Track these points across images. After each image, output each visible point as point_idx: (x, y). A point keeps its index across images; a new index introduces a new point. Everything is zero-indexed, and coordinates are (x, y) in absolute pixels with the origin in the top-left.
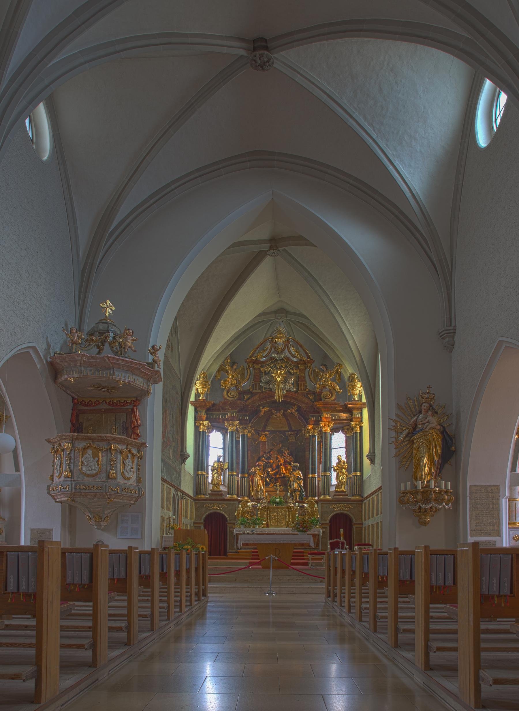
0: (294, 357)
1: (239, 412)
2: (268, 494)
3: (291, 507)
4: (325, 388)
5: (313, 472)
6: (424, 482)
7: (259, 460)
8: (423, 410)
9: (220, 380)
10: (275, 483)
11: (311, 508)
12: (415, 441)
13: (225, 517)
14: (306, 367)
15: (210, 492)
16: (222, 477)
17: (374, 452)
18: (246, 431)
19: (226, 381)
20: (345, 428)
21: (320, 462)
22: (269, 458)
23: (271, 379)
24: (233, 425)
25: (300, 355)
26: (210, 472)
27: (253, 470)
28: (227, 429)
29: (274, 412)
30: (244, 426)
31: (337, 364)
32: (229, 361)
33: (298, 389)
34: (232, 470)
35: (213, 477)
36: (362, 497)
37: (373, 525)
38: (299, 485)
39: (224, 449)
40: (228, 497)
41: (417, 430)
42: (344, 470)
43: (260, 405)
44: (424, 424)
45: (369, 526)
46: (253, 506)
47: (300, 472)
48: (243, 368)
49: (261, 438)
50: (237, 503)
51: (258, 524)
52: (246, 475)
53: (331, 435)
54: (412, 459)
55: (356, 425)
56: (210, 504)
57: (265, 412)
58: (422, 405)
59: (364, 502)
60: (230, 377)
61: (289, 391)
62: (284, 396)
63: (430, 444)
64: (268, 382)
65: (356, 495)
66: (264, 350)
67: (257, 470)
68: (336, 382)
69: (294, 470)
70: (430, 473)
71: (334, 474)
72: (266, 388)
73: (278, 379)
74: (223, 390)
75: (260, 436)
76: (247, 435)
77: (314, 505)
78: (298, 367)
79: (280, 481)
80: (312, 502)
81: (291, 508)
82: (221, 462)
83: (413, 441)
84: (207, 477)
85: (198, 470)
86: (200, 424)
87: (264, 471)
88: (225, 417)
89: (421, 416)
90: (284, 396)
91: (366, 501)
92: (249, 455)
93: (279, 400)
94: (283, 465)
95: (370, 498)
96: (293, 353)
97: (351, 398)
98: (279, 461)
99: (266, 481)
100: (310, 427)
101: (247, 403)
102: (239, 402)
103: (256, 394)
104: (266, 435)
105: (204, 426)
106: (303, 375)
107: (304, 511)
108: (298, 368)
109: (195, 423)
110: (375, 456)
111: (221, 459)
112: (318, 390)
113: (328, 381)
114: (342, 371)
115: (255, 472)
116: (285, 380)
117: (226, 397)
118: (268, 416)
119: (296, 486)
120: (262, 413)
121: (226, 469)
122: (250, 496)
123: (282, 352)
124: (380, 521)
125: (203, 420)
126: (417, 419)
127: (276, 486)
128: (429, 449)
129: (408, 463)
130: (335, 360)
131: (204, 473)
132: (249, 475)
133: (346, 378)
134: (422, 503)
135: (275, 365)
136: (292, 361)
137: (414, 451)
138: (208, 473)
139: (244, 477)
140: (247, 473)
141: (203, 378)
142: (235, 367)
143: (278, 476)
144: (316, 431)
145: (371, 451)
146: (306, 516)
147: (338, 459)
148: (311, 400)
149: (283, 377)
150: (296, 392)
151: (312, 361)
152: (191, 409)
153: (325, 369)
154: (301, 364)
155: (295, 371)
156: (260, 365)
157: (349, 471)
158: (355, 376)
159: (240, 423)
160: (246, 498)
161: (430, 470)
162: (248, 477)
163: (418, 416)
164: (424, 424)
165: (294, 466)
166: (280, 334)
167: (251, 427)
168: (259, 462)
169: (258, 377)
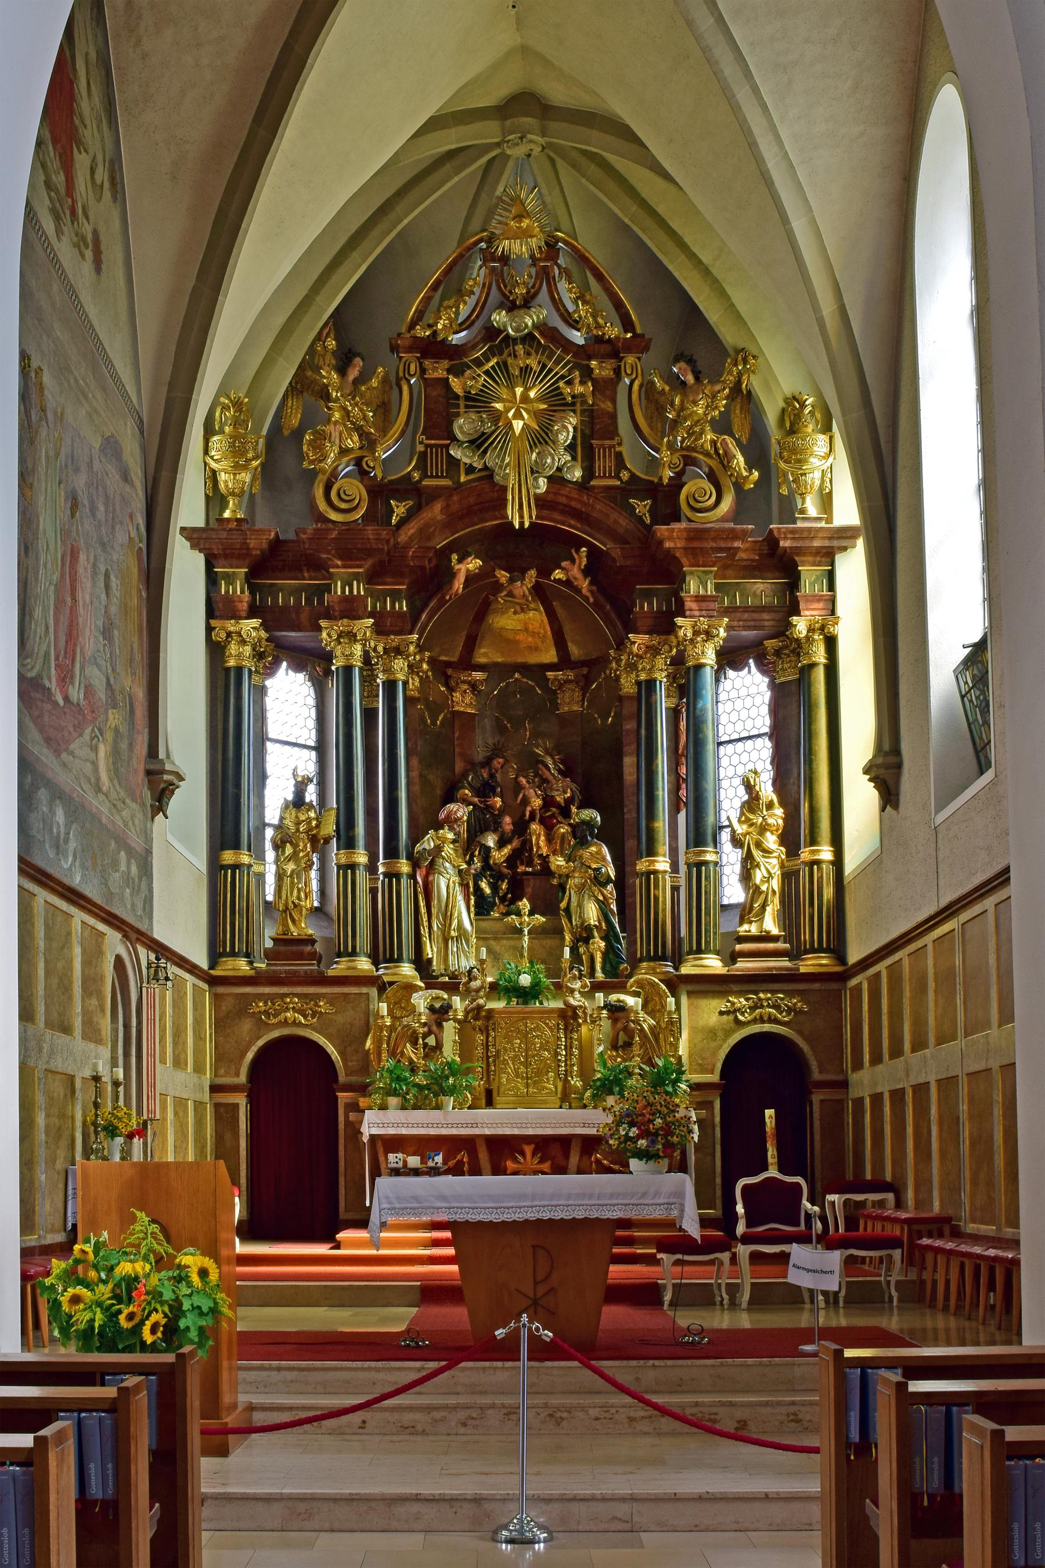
0: (574, 324)
1: (372, 578)
2: (489, 951)
3: (574, 1009)
4: (694, 462)
5: (651, 852)
7: (449, 797)
9: (298, 434)
10: (513, 901)
11: (651, 1014)
13: (328, 1056)
14: (617, 371)
15: (269, 944)
16: (313, 874)
18: (400, 665)
19: (321, 437)
20: (770, 644)
21: (676, 806)
22: (485, 790)
23: (489, 427)
24: (352, 637)
25: (594, 317)
26: (270, 855)
27: (428, 843)
28: (327, 657)
29: (503, 576)
30: (395, 640)
31: (738, 351)
32: (331, 344)
33: (589, 473)
34: (348, 843)
35: (280, 876)
38: (603, 905)
39: (320, 748)
40: (340, 967)
42: (771, 841)
43: (450, 548)
46: (431, 1009)
47: (605, 850)
48: (385, 381)
49: (457, 695)
50: (374, 992)
51: (452, 1091)
52: (404, 867)
53: (717, 680)
55: (811, 630)
56: (272, 997)
57: (470, 579)
60: (337, 415)
61: (556, 480)
62: (541, 502)
64: (479, 443)
65: (821, 950)
66: (460, 293)
67: (444, 840)
68: (732, 436)
69: (583, 843)
71: (731, 858)
72: (470, 469)
73: (518, 425)
74: (313, 474)
75: (451, 690)
76: (405, 683)
77: (662, 997)
78: (587, 374)
79: (529, 890)
80: (653, 985)
81: (575, 1016)
82: (310, 806)
84: (261, 877)
85: (223, 848)
86: (229, 634)
87: (469, 845)
88: (321, 601)
90: (541, 502)
92: (415, 774)
93: (522, 523)
94: (543, 822)
95: (881, 967)
96: (571, 308)
97: (789, 510)
98: (526, 801)
99: (478, 890)
100: (638, 641)
101: (403, 537)
102: (370, 531)
103: (435, 494)
104: (473, 686)
105: (243, 642)
106: (608, 406)
107: (625, 1029)
108: (587, 374)
109: (209, 629)
111: (311, 794)
112: (668, 474)
113: (702, 432)
114: (755, 383)
115: (438, 849)
116: (541, 437)
117: (322, 505)
118: (483, 596)
119: (592, 913)
120: (459, 584)
121: (327, 841)
122: (422, 965)
123: (527, 303)
125: (236, 617)
127: (518, 914)
130: (729, 335)
131: (245, 859)
132: (415, 864)
133: (771, 416)
135: (505, 363)
136: (567, 345)
138: (261, 857)
139: (398, 876)
140: (410, 857)
141: (236, 423)
142: (353, 373)
143: (521, 869)
144: (660, 662)
146: (636, 1050)
147: (749, 787)
148: (640, 519)
149: (536, 414)
150: (583, 485)
151: (640, 344)
152: (186, 570)
153: (690, 379)
154: (602, 357)
155: (579, 389)
156: (446, 364)
157: (790, 840)
158: (803, 405)
159: (380, 630)
160: (407, 970)
162: (412, 876)
165: (583, 822)
166: (519, 217)
167: (421, 649)
168: (453, 807)
169: (438, 413)
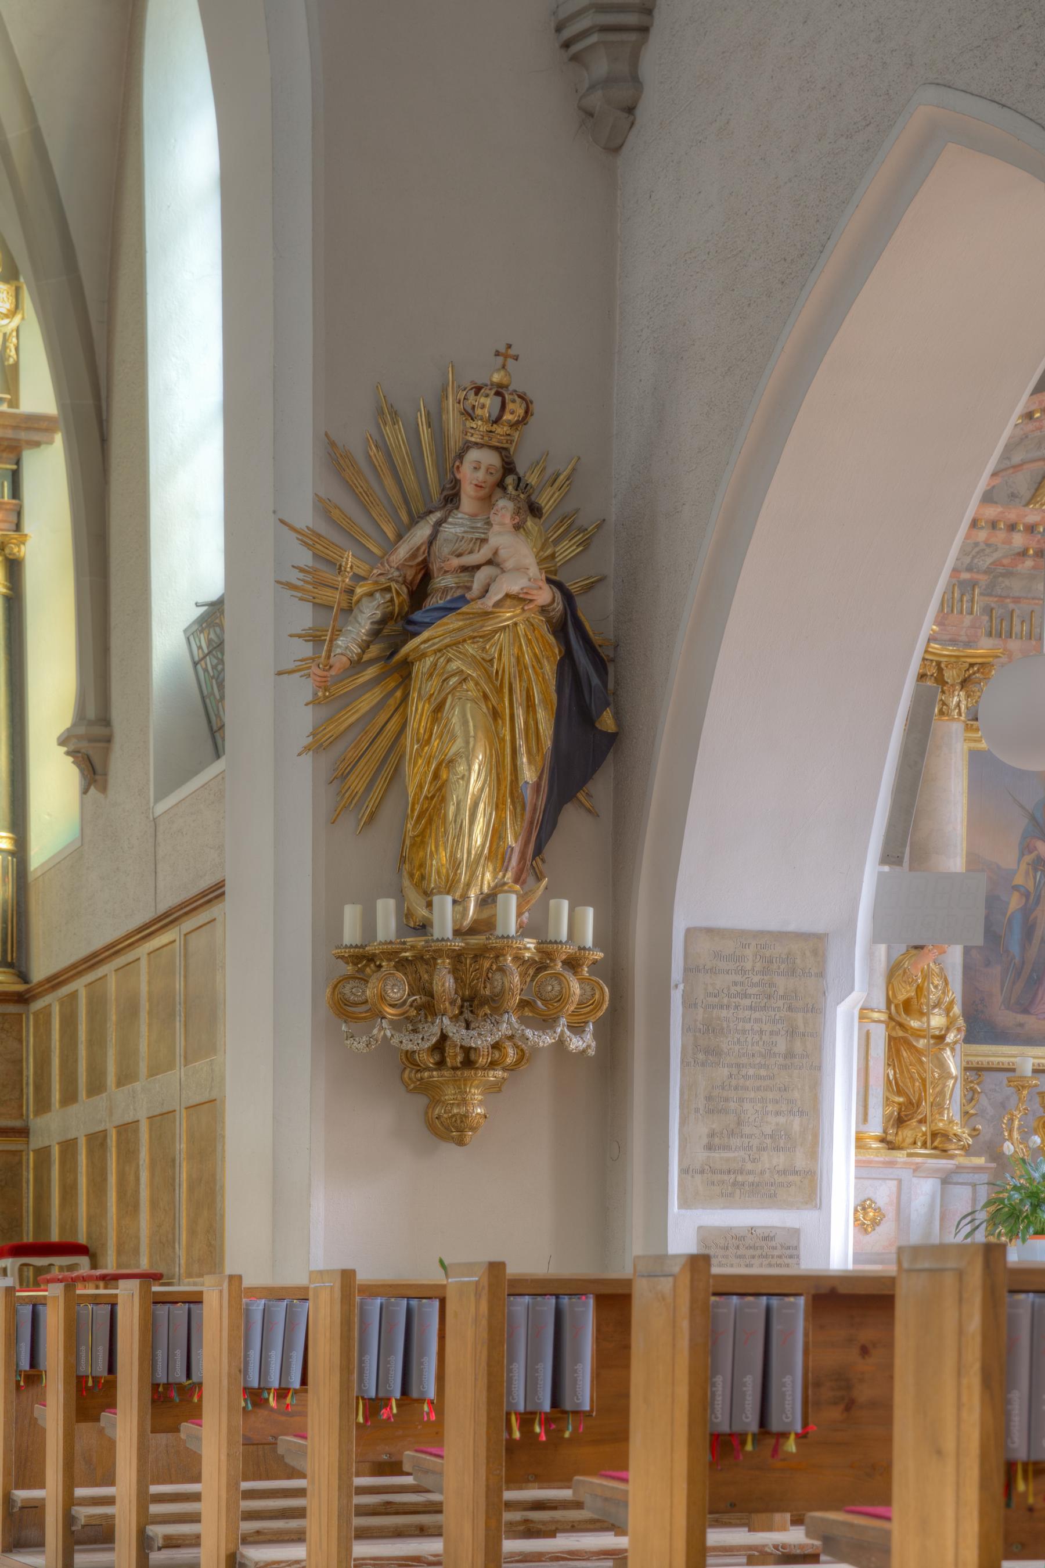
6: (465, 897)
8: (468, 491)
12: (421, 668)
17: (105, 720)
36: (23, 977)
37: (97, 1141)
41: (434, 601)
44: (472, 569)
45: (69, 1147)
54: (397, 770)
58: (460, 457)
59: (38, 1005)
63: (499, 691)
70: (496, 853)
83: (406, 665)
89: (455, 528)
91: (51, 1002)
95: (79, 985)
110: (108, 740)
124: (142, 1115)
126: (431, 541)
128: (496, 714)
129: (380, 785)
134: (455, 1019)
137: (412, 724)
145: (91, 713)
161: (496, 834)
163: (439, 523)
164: (472, 569)
